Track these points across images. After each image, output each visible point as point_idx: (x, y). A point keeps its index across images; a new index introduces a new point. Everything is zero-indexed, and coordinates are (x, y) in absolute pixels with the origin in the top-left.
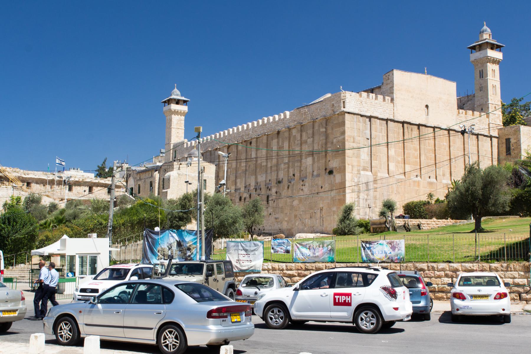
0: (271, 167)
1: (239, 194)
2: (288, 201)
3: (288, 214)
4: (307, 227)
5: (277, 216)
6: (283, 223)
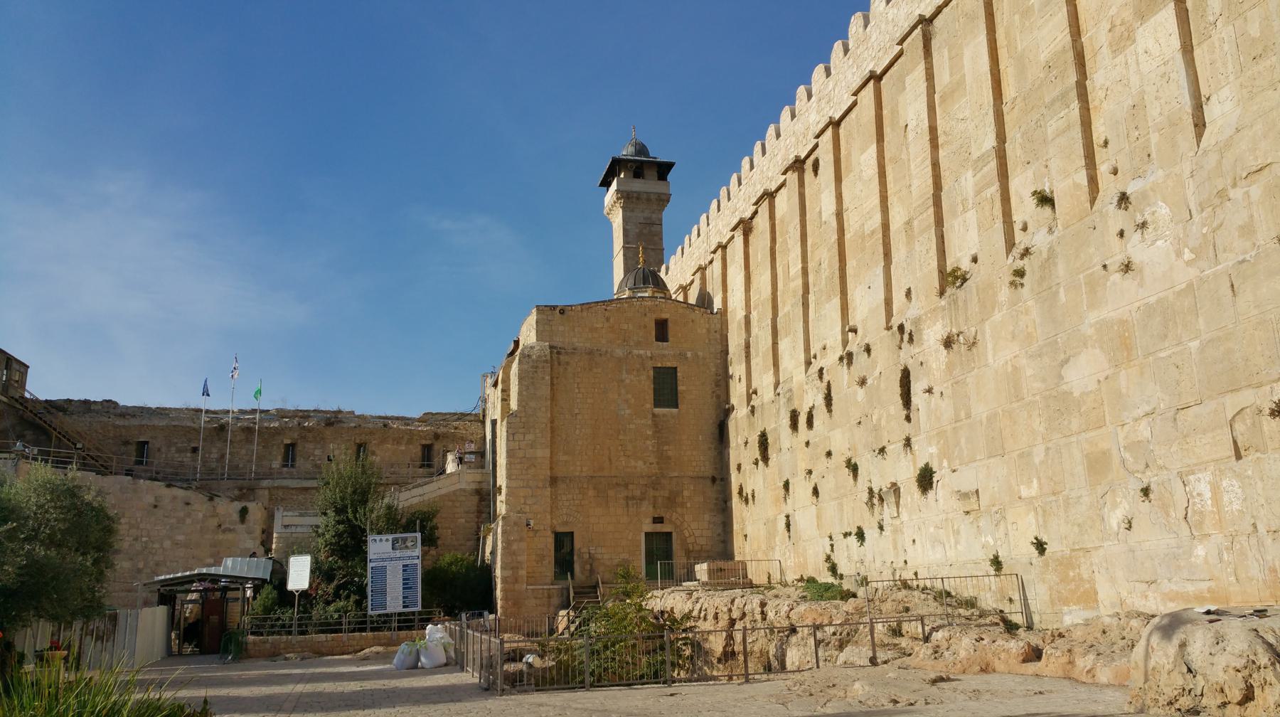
0: (909, 223)
1: (790, 400)
2: (1029, 372)
3: (1038, 455)
4: (1218, 538)
5: (967, 479)
6: (1010, 518)
